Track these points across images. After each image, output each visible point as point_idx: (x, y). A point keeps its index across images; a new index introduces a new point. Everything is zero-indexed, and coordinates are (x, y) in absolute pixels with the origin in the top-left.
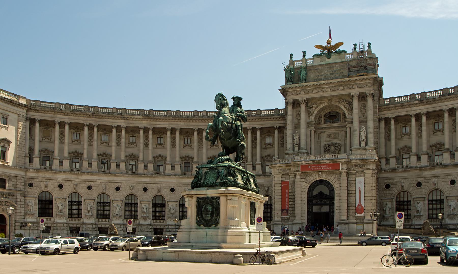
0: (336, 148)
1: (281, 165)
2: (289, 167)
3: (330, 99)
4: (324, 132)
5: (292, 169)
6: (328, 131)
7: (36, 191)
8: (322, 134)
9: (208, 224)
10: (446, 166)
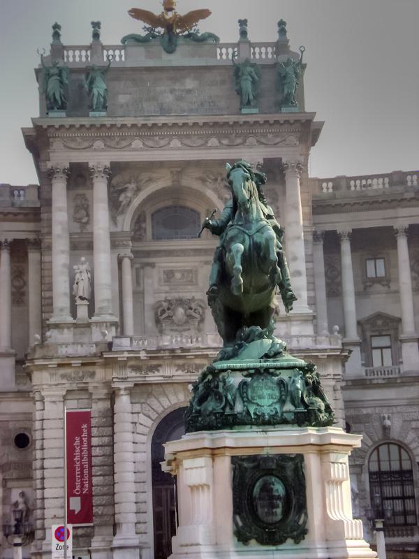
0: (192, 312)
1: (67, 362)
2: (90, 369)
3: (185, 165)
4: (152, 265)
5: (100, 373)
6: (164, 263)
8: (148, 269)
9: (271, 536)
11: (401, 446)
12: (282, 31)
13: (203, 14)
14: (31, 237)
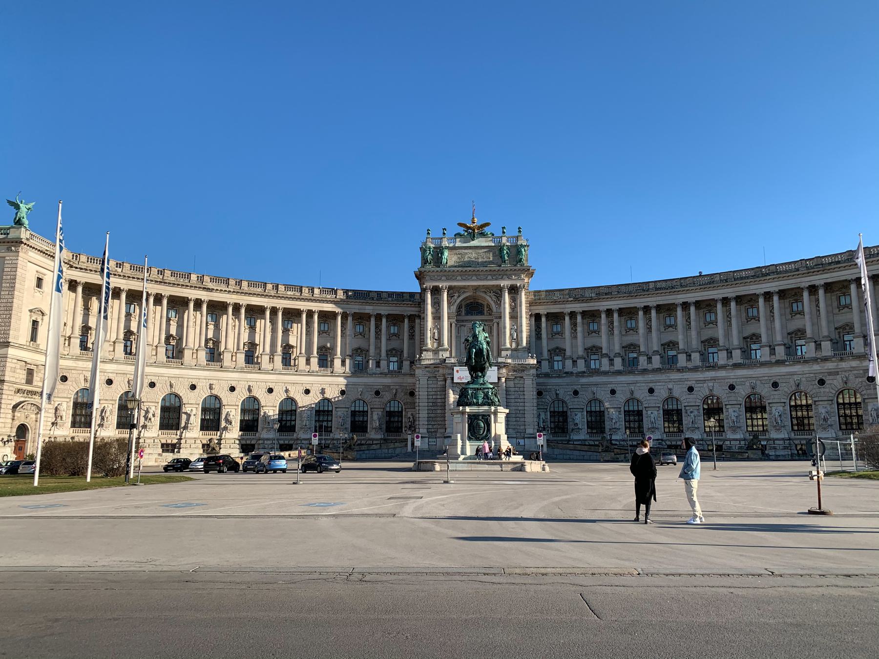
5: (441, 371)
7: (72, 388)
10: (606, 373)
11: (563, 402)
12: (520, 232)
13: (487, 224)
14: (417, 313)
